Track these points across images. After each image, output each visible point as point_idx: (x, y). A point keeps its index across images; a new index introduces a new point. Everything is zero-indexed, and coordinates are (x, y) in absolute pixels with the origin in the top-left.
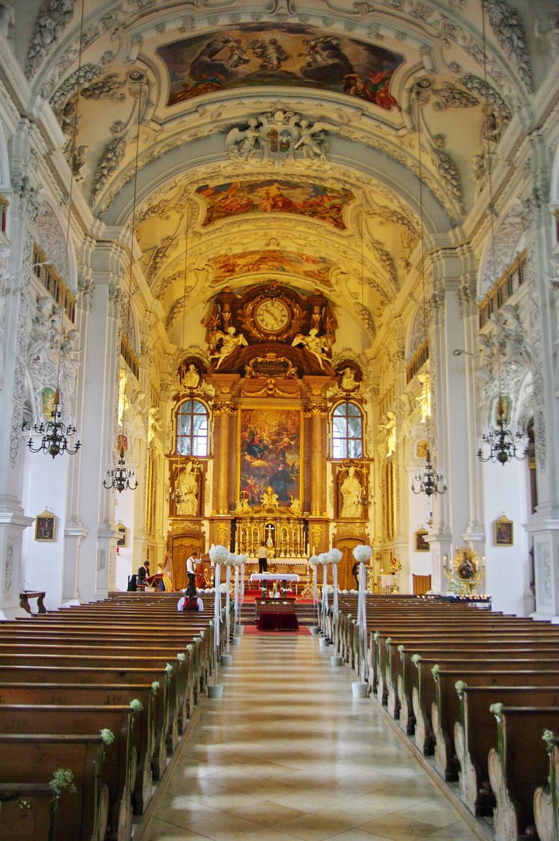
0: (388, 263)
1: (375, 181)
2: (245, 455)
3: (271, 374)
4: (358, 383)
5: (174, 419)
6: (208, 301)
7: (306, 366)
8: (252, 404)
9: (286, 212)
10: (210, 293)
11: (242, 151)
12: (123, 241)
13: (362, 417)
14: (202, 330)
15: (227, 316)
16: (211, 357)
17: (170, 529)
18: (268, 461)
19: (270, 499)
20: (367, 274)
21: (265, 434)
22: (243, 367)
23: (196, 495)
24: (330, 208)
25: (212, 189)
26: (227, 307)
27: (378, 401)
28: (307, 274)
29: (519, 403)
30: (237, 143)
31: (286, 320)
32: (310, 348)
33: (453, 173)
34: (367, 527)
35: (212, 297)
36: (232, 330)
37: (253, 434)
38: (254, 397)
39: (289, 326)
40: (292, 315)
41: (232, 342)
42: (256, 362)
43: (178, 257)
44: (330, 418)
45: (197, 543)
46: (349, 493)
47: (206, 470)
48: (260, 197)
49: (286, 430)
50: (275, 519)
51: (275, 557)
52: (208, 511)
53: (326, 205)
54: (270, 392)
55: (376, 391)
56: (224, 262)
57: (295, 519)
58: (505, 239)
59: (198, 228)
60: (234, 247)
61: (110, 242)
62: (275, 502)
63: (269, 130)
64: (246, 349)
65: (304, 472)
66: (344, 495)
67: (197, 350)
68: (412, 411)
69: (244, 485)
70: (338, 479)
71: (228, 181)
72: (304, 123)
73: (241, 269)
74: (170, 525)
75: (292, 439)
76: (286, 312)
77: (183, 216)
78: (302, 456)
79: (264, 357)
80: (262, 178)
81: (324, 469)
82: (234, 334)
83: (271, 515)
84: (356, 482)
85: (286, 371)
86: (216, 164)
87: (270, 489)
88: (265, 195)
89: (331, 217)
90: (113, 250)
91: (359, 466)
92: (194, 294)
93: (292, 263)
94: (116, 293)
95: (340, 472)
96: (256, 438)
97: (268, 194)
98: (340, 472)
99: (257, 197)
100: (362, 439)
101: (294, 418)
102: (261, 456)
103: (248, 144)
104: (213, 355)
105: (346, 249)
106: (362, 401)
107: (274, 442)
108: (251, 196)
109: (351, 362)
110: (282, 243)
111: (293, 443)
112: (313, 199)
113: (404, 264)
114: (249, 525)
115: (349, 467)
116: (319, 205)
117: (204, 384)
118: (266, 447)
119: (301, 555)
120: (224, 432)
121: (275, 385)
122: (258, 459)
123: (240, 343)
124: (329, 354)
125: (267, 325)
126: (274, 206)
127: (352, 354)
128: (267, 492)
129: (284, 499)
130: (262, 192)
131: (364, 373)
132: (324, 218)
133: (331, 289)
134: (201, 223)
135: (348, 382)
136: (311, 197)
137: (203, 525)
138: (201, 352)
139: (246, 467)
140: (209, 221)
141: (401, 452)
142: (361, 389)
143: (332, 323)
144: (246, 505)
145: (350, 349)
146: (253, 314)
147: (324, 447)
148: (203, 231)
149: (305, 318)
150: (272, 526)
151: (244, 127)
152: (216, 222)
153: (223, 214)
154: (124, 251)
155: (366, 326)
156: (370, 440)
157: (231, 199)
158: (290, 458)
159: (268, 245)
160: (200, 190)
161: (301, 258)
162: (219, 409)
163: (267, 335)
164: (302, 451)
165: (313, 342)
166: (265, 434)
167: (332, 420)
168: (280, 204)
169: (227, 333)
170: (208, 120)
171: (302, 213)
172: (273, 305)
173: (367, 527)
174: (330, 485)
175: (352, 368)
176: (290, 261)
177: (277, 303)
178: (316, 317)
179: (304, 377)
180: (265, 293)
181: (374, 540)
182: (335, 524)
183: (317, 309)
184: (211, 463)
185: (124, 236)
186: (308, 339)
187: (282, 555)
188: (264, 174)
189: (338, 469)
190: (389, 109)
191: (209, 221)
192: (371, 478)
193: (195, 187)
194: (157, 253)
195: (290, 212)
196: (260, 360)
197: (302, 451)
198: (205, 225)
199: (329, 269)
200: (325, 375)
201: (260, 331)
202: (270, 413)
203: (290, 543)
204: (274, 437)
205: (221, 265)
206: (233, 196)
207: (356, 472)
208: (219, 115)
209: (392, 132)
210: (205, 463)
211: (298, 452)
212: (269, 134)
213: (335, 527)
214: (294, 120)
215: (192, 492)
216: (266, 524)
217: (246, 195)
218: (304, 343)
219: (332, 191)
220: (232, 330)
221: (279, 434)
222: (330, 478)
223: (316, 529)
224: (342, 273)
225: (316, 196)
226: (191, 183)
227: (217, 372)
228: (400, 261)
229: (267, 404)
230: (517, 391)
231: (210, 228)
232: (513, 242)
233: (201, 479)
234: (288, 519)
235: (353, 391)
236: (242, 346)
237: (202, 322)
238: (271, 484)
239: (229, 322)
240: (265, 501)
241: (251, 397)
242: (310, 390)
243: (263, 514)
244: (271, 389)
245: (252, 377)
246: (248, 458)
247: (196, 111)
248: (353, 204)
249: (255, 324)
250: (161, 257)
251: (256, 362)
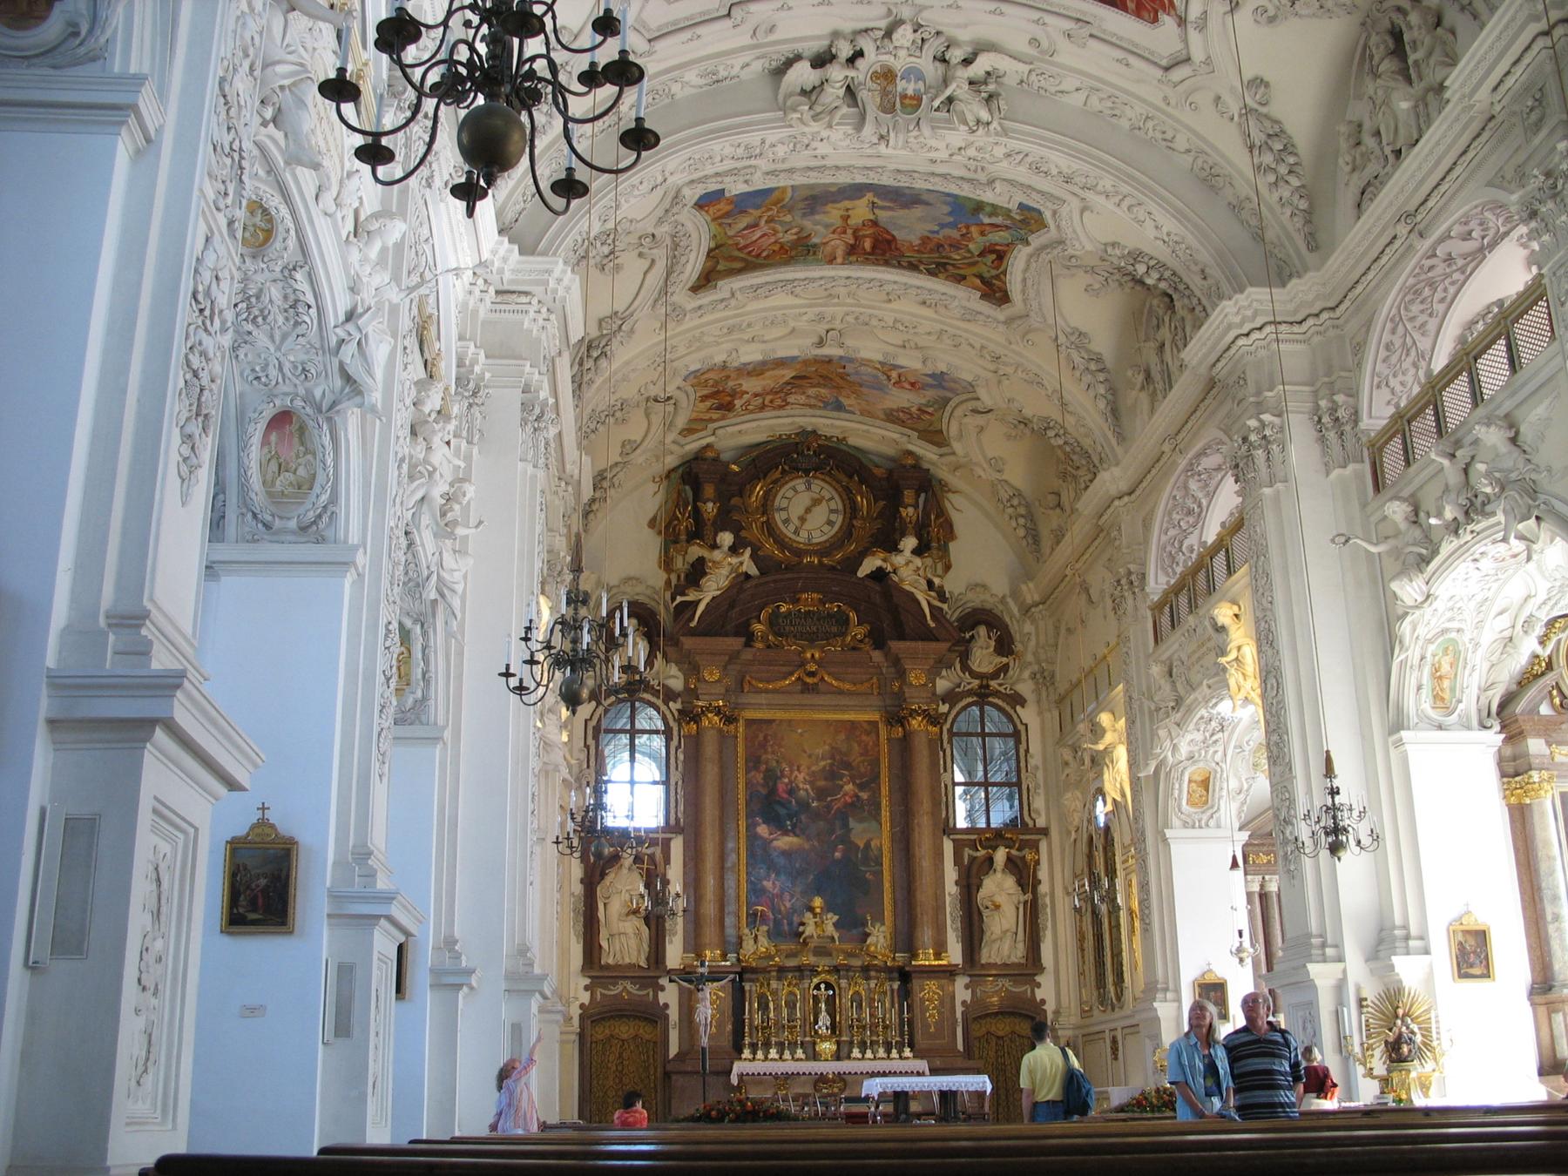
0: (1101, 377)
1: (1107, 183)
2: (755, 825)
3: (812, 639)
4: (1005, 660)
5: (591, 742)
7: (890, 616)
8: (770, 706)
9: (876, 263)
10: (671, 461)
11: (818, 109)
12: (555, 291)
13: (1016, 735)
14: (652, 544)
15: (710, 508)
16: (679, 599)
17: (585, 998)
18: (808, 839)
19: (821, 925)
20: (1036, 406)
21: (801, 777)
22: (748, 624)
23: (647, 920)
24: (981, 255)
25: (730, 201)
26: (709, 491)
27: (1053, 697)
28: (892, 417)
29: (1480, 652)
30: (804, 92)
31: (838, 520)
32: (902, 580)
33: (1292, 160)
34: (1039, 985)
35: (674, 470)
36: (726, 538)
37: (772, 777)
38: (775, 691)
39: (847, 533)
40: (852, 510)
41: (726, 566)
42: (776, 614)
43: (627, 363)
44: (945, 736)
45: (645, 1031)
46: (997, 907)
47: (667, 861)
48: (827, 226)
49: (848, 766)
50: (836, 970)
51: (837, 1057)
52: (674, 955)
53: (971, 246)
54: (809, 680)
55: (1044, 679)
56: (716, 383)
57: (879, 969)
58: (1427, 292)
59: (681, 296)
61: (526, 293)
62: (830, 929)
63: (877, 68)
64: (754, 582)
65: (892, 860)
66: (985, 913)
67: (640, 589)
68: (1179, 701)
69: (756, 891)
70: (968, 876)
71: (771, 183)
72: (956, 55)
73: (748, 403)
74: (586, 988)
75: (862, 787)
76: (837, 504)
77: (653, 261)
78: (886, 826)
79: (796, 601)
80: (844, 179)
81: (939, 854)
82: (730, 549)
83: (823, 963)
84: (1010, 882)
85: (844, 634)
86: (754, 138)
87: (818, 902)
88: (839, 223)
89: (980, 277)
90: (532, 314)
91: (1017, 844)
92: (639, 458)
93: (864, 390)
94: (537, 411)
95: (973, 859)
96: (781, 787)
97: (846, 218)
98: (973, 859)
99: (821, 227)
100: (1019, 784)
101: (864, 738)
102: (794, 826)
103: (835, 92)
104: (683, 594)
105: (1000, 351)
106: (1017, 700)
107: (821, 794)
108: (808, 224)
109: (989, 612)
110: (849, 342)
111: (864, 795)
112: (947, 232)
113: (1141, 378)
114: (774, 984)
115: (995, 848)
116: (955, 246)
117: (659, 662)
118: (804, 806)
119: (900, 1052)
120: (710, 773)
121: (819, 663)
122: (786, 833)
123: (744, 568)
124: (942, 596)
125: (796, 532)
126: (854, 252)
127: (987, 597)
128: (811, 909)
129: (853, 925)
130: (833, 214)
131: (1017, 637)
132: (960, 279)
133: (944, 450)
134: (690, 285)
135: (983, 657)
136: (942, 226)
137: (662, 989)
138: (649, 592)
139: (758, 853)
140: (706, 281)
141: (1147, 798)
142: (1011, 672)
143: (941, 525)
144: (763, 940)
145: (984, 586)
146: (766, 506)
147: (936, 803)
148: (690, 302)
149: (880, 515)
150: (829, 986)
151: (822, 60)
152: (720, 283)
153: (738, 265)
154: (553, 317)
155: (1021, 532)
156: (1037, 787)
157: (765, 227)
158: (859, 832)
159: (821, 343)
160: (702, 204)
161: (891, 375)
162: (696, 719)
163: (799, 553)
164: (885, 814)
165: (906, 566)
166: (801, 777)
167: (950, 742)
168: (868, 245)
169: (714, 546)
170: (746, 40)
171: (913, 267)
172: (809, 488)
173: (1039, 985)
174: (951, 888)
175: (990, 626)
176: (856, 387)
177: (817, 485)
178: (908, 512)
179: (895, 645)
180: (793, 460)
181: (1057, 1012)
182: (967, 980)
183: (908, 495)
184: (677, 846)
185: (559, 281)
186: (898, 560)
187: (856, 1053)
188: (848, 168)
189: (967, 852)
190: (1155, 20)
191: (706, 281)
192: (1043, 874)
193: (700, 190)
194: (589, 348)
195: (887, 263)
196: (783, 610)
197: (885, 814)
198: (695, 289)
199: (947, 401)
200: (937, 640)
201: (781, 543)
202: (813, 725)
203: (873, 1026)
204: (821, 783)
205: (705, 392)
206: (770, 220)
207: (1009, 859)
208: (772, 29)
209: (1159, 73)
210: (666, 845)
211: (876, 816)
212: (875, 76)
213: (967, 987)
214: (934, 46)
215: (636, 912)
216: (816, 981)
217: (799, 220)
218: (889, 569)
219: (995, 210)
220: (726, 538)
221: (832, 775)
222: (951, 874)
223: (928, 990)
224: (975, 411)
225: (953, 225)
226: (692, 182)
227: (693, 633)
228: (1129, 373)
229: (802, 707)
230: (1479, 625)
231: (706, 298)
232: (1442, 300)
233: (654, 878)
234: (866, 970)
235: (995, 675)
236: (747, 576)
237: (652, 523)
238: (819, 893)
239: (714, 523)
240: (810, 930)
241: (767, 691)
242: (902, 674)
243: (808, 959)
244: (812, 674)
245: (769, 647)
246: (763, 830)
247: (729, 15)
248: (1036, 240)
249: (770, 529)
250: (596, 359)
251: (776, 614)
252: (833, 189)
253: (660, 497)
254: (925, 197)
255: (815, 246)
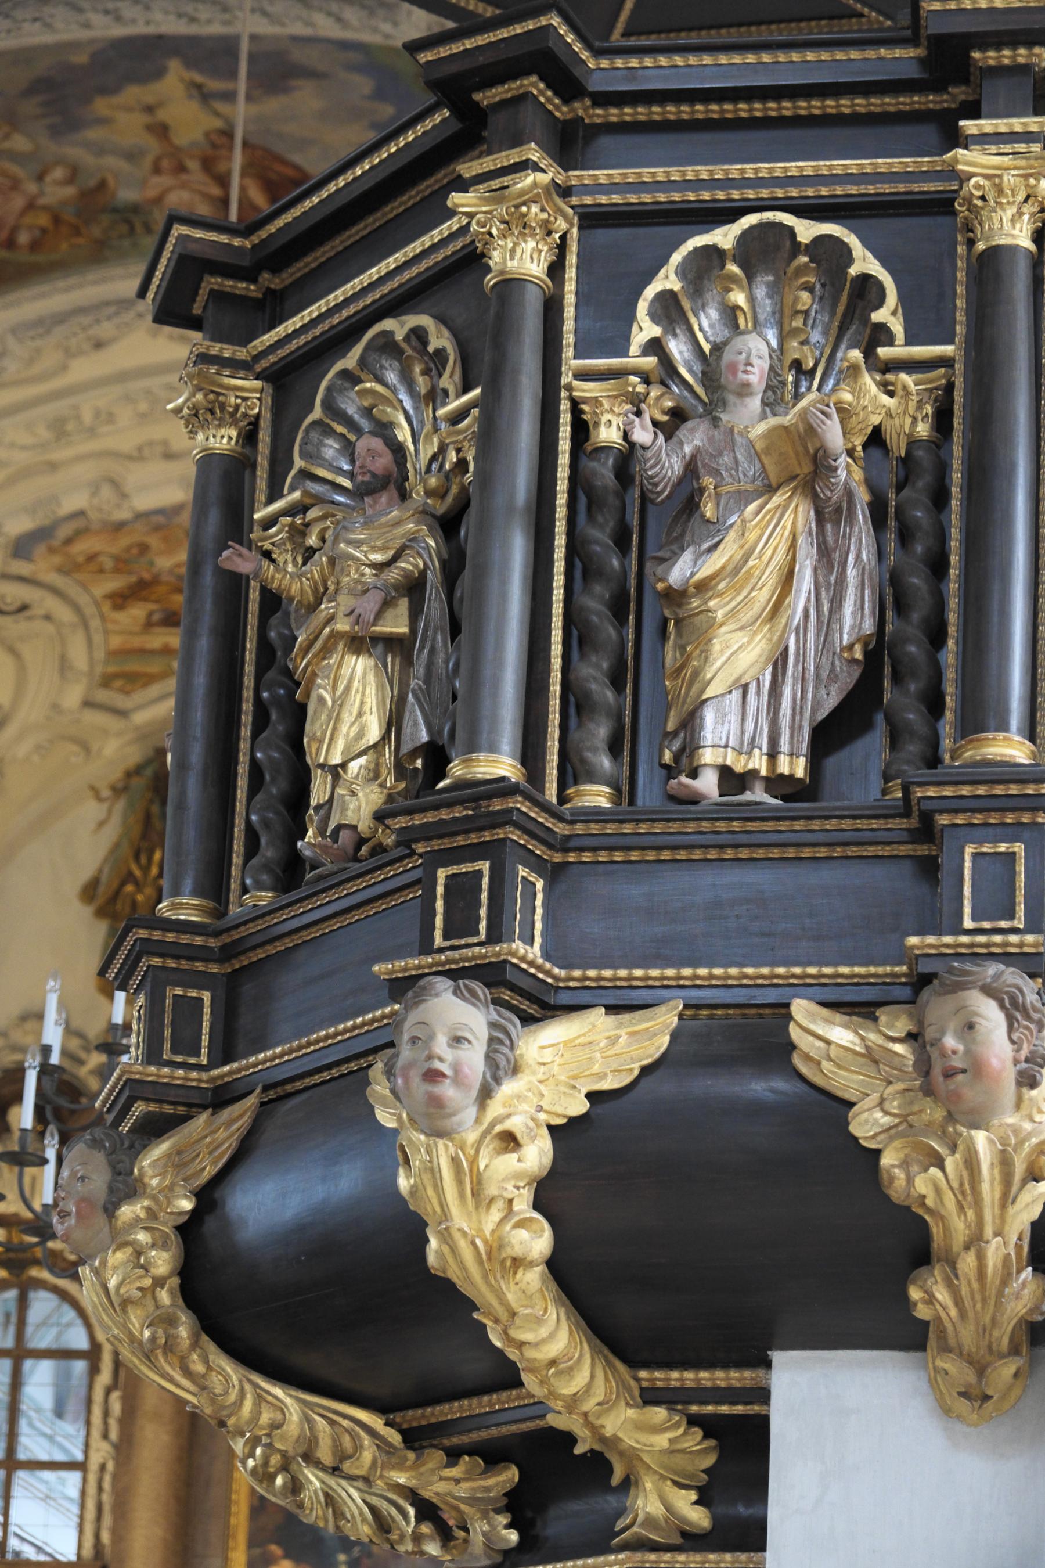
6: (118, 791)
48: (132, 156)
56: (122, 564)
60: (134, 476)
88: (153, 146)
97: (162, 131)
108: (73, 152)
130: (121, 118)
205: (114, 584)
237: (89, 892)
252: (81, 58)
253: (111, 833)
254: (299, 56)
255: (135, 209)
